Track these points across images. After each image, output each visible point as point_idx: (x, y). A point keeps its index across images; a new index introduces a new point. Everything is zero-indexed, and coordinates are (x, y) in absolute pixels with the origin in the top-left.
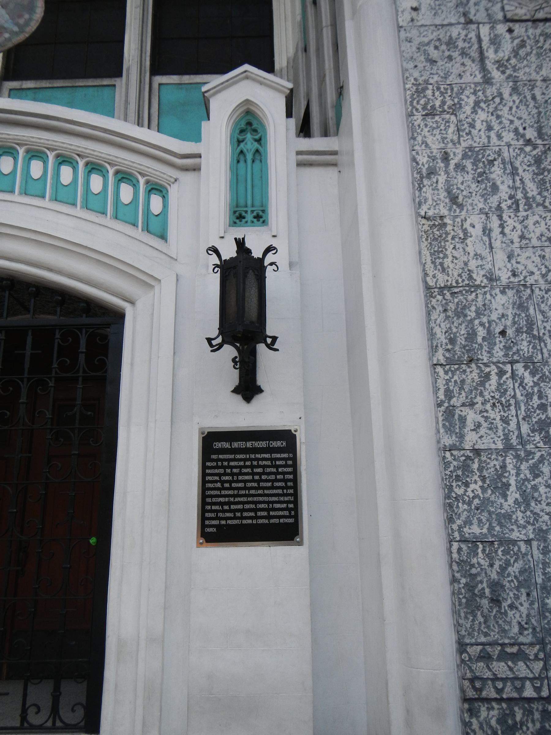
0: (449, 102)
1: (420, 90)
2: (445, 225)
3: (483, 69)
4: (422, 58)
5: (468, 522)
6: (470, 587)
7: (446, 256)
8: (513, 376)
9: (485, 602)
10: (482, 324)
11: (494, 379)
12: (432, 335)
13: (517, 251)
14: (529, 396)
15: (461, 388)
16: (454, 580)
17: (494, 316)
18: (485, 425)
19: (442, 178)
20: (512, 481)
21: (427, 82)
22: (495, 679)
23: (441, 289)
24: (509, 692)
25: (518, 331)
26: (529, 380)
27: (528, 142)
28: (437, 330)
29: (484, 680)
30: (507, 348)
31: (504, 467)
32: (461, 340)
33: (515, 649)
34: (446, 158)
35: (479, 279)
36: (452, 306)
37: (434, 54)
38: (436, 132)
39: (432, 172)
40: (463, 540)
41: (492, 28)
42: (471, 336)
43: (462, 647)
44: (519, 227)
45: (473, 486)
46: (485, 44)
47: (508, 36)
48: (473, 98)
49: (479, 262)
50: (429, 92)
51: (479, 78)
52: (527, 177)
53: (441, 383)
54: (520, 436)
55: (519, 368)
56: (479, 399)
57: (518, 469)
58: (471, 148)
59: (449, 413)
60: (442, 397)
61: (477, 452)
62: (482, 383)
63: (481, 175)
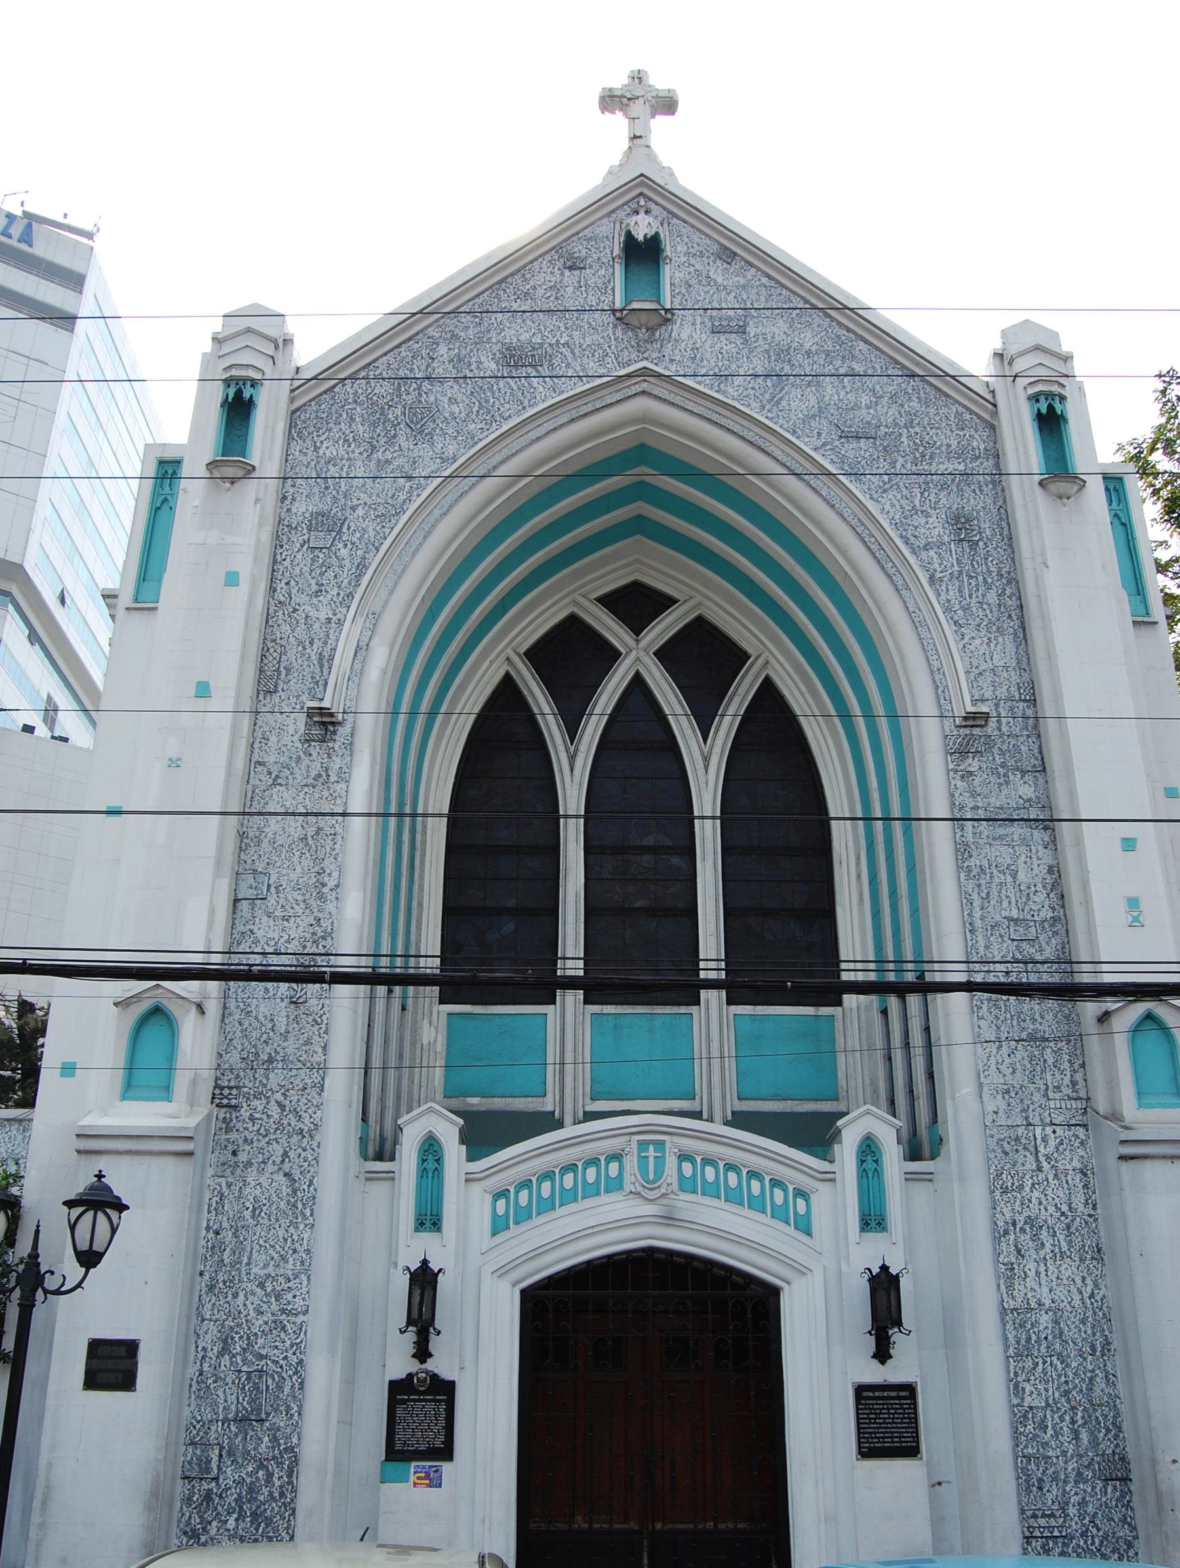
0: (1017, 1184)
1: (999, 1175)
2: (1014, 1269)
3: (1037, 1160)
4: (1000, 1150)
5: (1026, 1447)
6: (1027, 1481)
7: (1014, 1289)
8: (1051, 1364)
9: (1035, 1489)
10: (1034, 1333)
11: (1041, 1365)
12: (1006, 1339)
13: (1055, 1287)
14: (1059, 1376)
15: (1023, 1371)
16: (1018, 1478)
17: (1041, 1328)
18: (1035, 1392)
19: (1012, 1237)
20: (1050, 1425)
21: (1002, 1168)
22: (1040, 1527)
23: (1012, 1310)
24: (1047, 1534)
25: (1054, 1337)
26: (1059, 1366)
27: (1063, 1214)
28: (1009, 1336)
29: (1034, 1528)
30: (1048, 1347)
31: (1045, 1416)
32: (1023, 1342)
33: (1049, 1512)
34: (1014, 1224)
35: (1033, 1305)
36: (1018, 1321)
37: (1007, 1147)
38: (1009, 1205)
39: (1006, 1233)
40: (1024, 1456)
41: (1043, 1129)
42: (1029, 1340)
43: (1023, 1511)
44: (1056, 1271)
45: (1029, 1427)
46: (1039, 1141)
47: (1053, 1136)
48: (1031, 1180)
49: (1034, 1294)
50: (1004, 1176)
51: (1034, 1167)
52: (1062, 1237)
53: (1012, 1368)
54: (1054, 1399)
55: (1054, 1359)
56: (1032, 1378)
57: (1053, 1417)
58: (1029, 1217)
59: (1016, 1386)
60: (1012, 1376)
61: (1031, 1408)
62: (1034, 1368)
63: (1035, 1235)
